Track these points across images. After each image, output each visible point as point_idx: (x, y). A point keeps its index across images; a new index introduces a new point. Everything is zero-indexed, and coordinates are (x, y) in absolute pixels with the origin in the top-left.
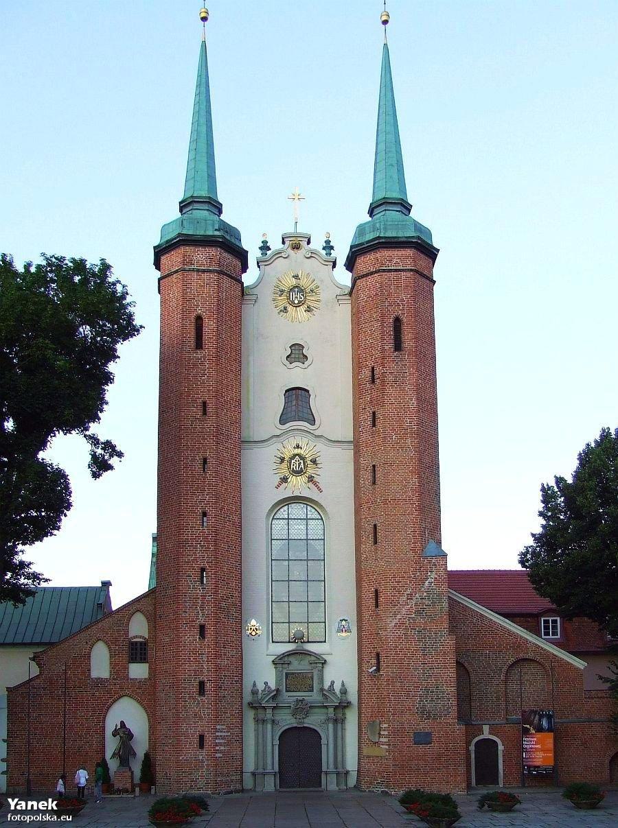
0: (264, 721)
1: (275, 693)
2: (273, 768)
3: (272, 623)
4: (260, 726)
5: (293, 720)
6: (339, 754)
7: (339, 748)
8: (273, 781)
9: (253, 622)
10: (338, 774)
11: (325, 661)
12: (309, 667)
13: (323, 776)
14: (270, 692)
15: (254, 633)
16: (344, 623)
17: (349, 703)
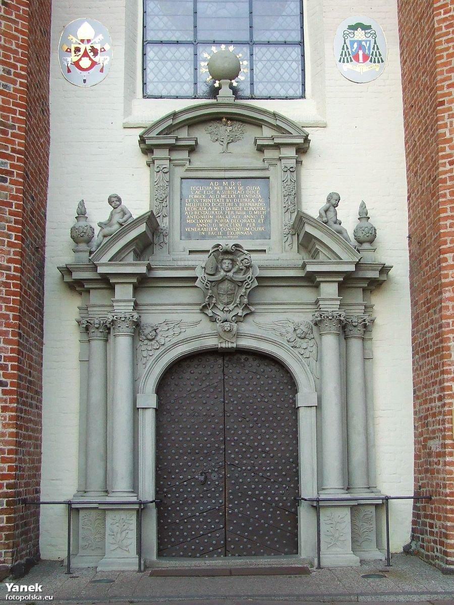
0: (108, 329)
1: (142, 228)
2: (135, 489)
3: (145, 43)
4: (97, 345)
5: (206, 327)
6: (357, 440)
7: (357, 421)
8: (133, 535)
9: (85, 31)
10: (356, 508)
11: (307, 140)
12: (256, 161)
13: (305, 517)
14: (125, 228)
15: (85, 63)
16: (360, 34)
17: (384, 269)
